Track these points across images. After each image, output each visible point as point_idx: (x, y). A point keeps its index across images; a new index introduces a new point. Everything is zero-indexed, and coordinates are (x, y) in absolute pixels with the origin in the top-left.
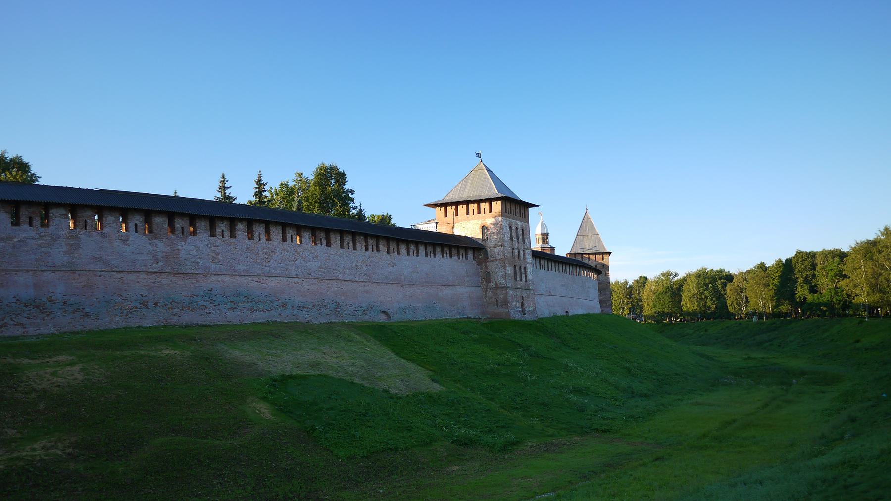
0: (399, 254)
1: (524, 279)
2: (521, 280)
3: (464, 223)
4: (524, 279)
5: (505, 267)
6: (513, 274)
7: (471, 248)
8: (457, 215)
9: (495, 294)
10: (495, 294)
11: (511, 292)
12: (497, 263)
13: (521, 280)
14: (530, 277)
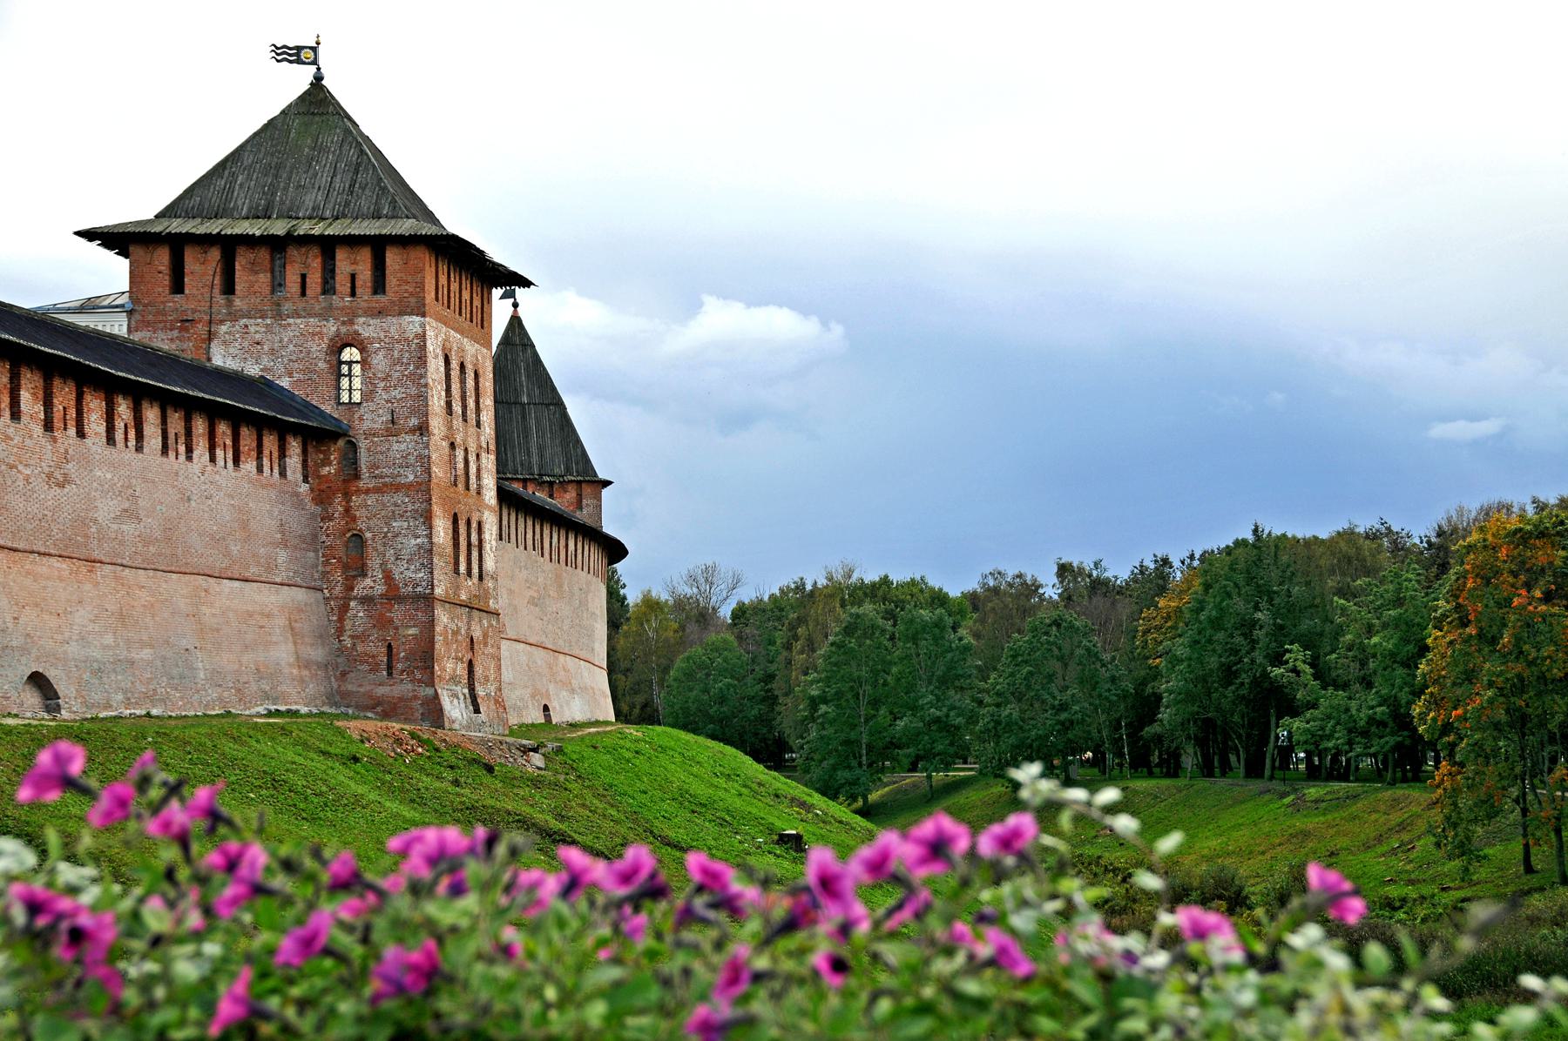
0: (81, 434)
1: (475, 570)
2: (469, 573)
3: (256, 327)
4: (475, 570)
5: (428, 518)
6: (449, 550)
7: (297, 430)
8: (229, 288)
9: (383, 623)
10: (383, 623)
11: (443, 617)
12: (399, 498)
13: (469, 573)
14: (490, 564)
